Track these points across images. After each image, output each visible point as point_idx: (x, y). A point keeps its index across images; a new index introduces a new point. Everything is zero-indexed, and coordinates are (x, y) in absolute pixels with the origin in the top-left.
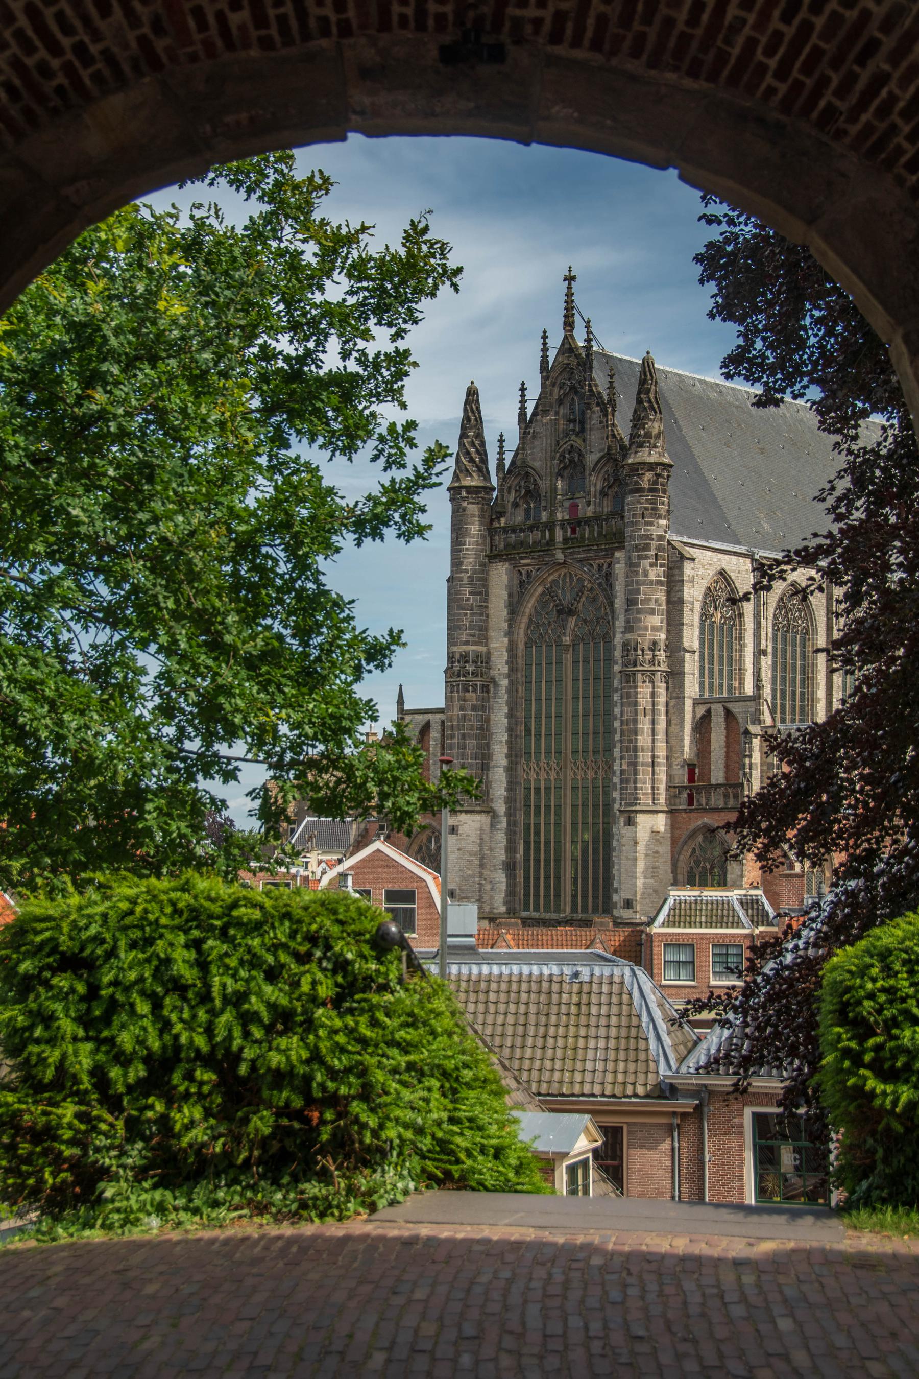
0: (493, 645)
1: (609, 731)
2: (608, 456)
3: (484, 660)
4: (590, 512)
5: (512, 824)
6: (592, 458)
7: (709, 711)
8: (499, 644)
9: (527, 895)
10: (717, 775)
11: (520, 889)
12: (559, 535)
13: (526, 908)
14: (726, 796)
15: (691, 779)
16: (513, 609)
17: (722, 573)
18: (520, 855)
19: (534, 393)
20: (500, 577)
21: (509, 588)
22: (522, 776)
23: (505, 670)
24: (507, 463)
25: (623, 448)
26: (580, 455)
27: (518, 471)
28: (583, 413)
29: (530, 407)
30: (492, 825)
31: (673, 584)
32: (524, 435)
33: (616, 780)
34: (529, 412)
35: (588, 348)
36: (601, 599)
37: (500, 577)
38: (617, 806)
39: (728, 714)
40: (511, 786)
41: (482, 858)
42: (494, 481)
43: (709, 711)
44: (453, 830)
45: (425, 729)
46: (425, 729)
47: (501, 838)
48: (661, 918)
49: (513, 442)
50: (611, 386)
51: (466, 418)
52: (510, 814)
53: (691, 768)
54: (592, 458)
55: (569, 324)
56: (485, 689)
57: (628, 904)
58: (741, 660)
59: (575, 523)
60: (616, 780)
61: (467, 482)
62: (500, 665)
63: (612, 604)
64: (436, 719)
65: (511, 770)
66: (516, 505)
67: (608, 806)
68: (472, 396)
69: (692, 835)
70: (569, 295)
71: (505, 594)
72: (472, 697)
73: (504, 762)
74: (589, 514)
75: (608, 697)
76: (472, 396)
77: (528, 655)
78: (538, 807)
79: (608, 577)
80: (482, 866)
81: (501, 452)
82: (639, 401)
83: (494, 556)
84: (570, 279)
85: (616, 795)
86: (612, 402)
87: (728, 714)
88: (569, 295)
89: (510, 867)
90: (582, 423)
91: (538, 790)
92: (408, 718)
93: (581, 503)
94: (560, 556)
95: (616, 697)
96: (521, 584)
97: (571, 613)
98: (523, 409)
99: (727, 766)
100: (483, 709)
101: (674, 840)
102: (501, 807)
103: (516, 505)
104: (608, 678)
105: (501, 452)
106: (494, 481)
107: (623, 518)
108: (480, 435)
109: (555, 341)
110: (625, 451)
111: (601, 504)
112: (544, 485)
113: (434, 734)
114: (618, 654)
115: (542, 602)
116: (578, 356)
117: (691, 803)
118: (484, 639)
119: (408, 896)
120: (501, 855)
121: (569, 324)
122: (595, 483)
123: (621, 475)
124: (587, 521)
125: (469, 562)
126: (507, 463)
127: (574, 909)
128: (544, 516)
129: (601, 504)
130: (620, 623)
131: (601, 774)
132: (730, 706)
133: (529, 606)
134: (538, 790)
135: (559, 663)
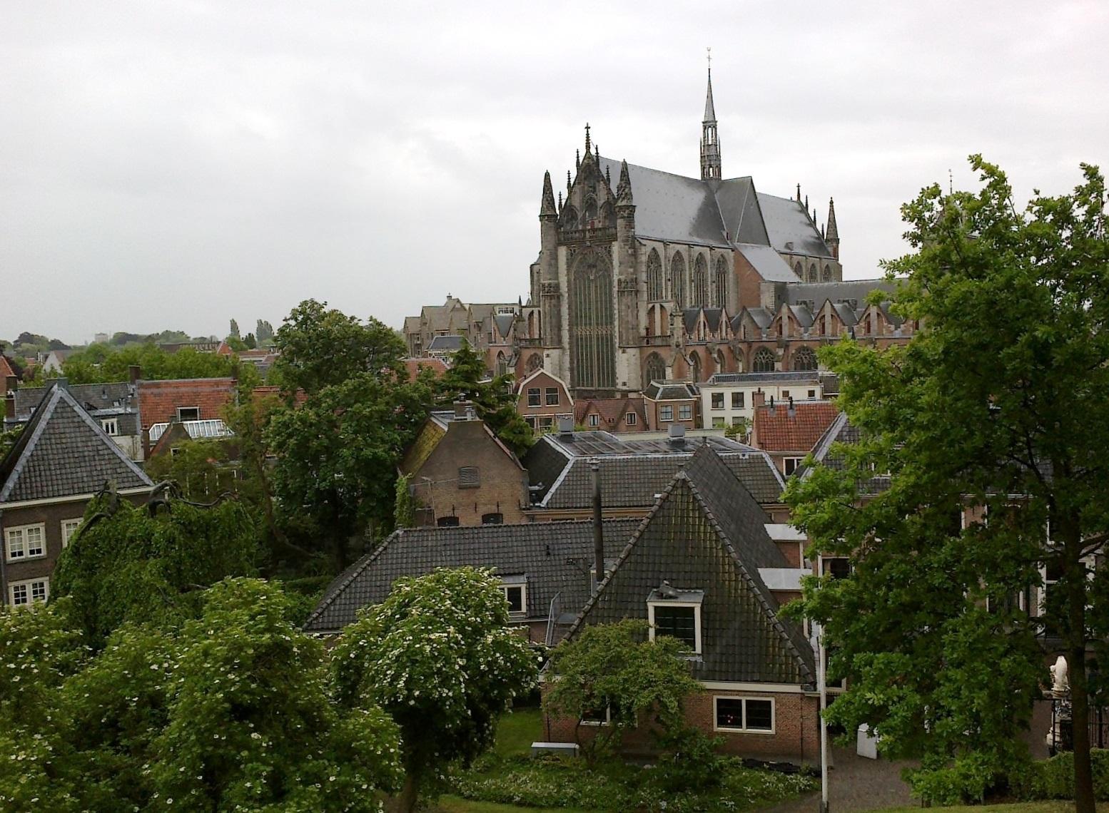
0: (561, 280)
1: (612, 316)
2: (608, 203)
3: (557, 286)
4: (600, 226)
5: (571, 352)
6: (600, 203)
7: (654, 306)
8: (563, 281)
9: (579, 380)
10: (658, 333)
11: (576, 379)
12: (588, 235)
13: (579, 386)
14: (663, 340)
15: (647, 334)
16: (569, 266)
17: (654, 249)
18: (575, 365)
19: (574, 174)
20: (563, 252)
21: (567, 256)
22: (575, 334)
23: (566, 290)
24: (563, 204)
25: (614, 198)
26: (595, 201)
27: (568, 208)
28: (594, 184)
29: (572, 183)
30: (563, 353)
31: (635, 255)
32: (570, 193)
33: (617, 334)
34: (572, 183)
35: (597, 157)
36: (607, 260)
37: (563, 252)
38: (617, 345)
39: (662, 307)
40: (571, 337)
41: (560, 366)
42: (558, 212)
43: (654, 306)
44: (548, 356)
45: (532, 312)
46: (532, 313)
47: (567, 359)
48: (658, 395)
49: (565, 195)
50: (608, 173)
51: (545, 186)
52: (570, 349)
53: (647, 329)
54: (600, 203)
55: (588, 147)
56: (558, 297)
57: (624, 384)
58: (661, 284)
59: (594, 230)
60: (617, 334)
61: (549, 213)
62: (564, 288)
63: (612, 263)
64: (536, 310)
65: (570, 330)
66: (567, 222)
67: (612, 346)
68: (547, 175)
69: (649, 356)
70: (588, 134)
71: (565, 259)
72: (553, 301)
73: (567, 328)
74: (600, 226)
75: (611, 301)
76: (547, 175)
77: (575, 284)
78: (582, 346)
79: (610, 253)
80: (560, 369)
81: (560, 200)
82: (621, 180)
83: (560, 244)
84: (588, 128)
85: (617, 340)
86: (609, 179)
87: (662, 307)
88: (588, 134)
89: (572, 370)
90: (595, 188)
91: (582, 339)
92: (524, 309)
93: (596, 222)
94: (588, 244)
95: (615, 301)
96: (572, 255)
97: (594, 266)
98: (569, 184)
99: (662, 327)
100: (558, 306)
101: (641, 359)
102: (567, 346)
103: (567, 222)
104: (611, 295)
105: (560, 200)
106: (558, 212)
107: (616, 228)
108: (552, 193)
109: (582, 153)
110: (616, 200)
111: (604, 222)
112: (580, 215)
113: (536, 315)
114: (616, 283)
115: (581, 262)
116: (593, 160)
117: (648, 342)
118: (557, 278)
119: (555, 390)
120: (567, 365)
121: (588, 147)
122: (601, 213)
123: (611, 209)
124: (600, 229)
125: (551, 246)
126: (563, 204)
127: (599, 386)
128: (580, 227)
129: (604, 222)
130: (616, 271)
131: (609, 332)
132: (664, 304)
133: (575, 265)
134: (582, 339)
135: (589, 287)
